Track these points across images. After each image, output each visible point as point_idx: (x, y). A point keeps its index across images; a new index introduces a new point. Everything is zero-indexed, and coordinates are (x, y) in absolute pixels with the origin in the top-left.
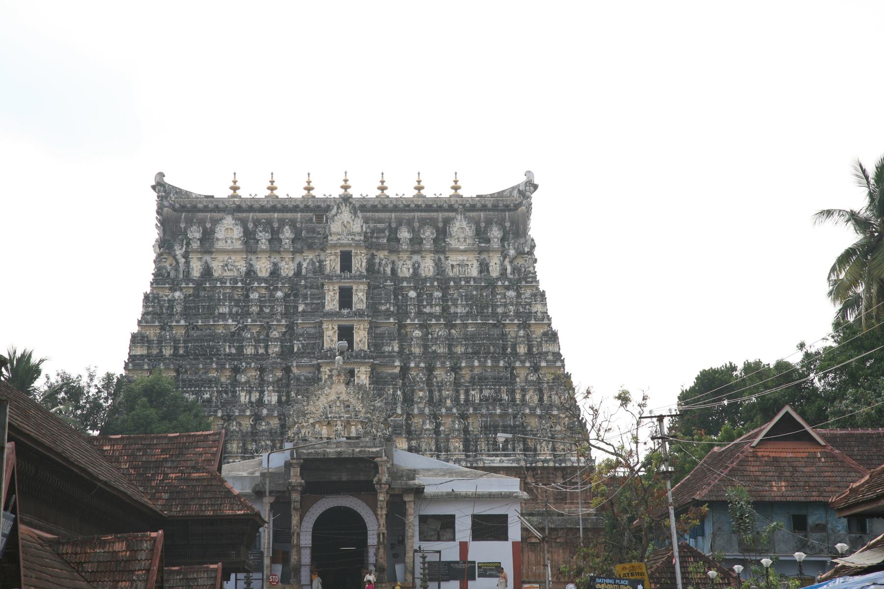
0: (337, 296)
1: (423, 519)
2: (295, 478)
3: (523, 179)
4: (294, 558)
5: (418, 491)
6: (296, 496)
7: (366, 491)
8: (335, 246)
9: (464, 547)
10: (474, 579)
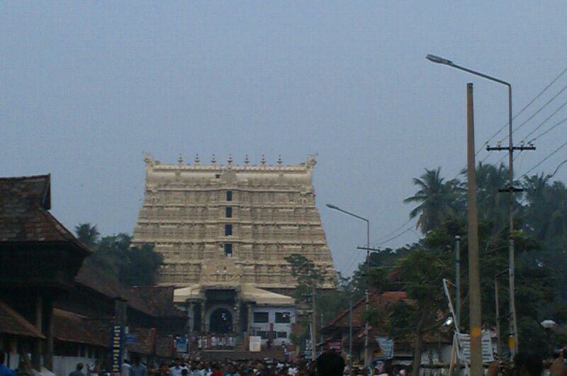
0: (225, 212)
1: (256, 314)
2: (202, 297)
3: (310, 159)
4: (202, 329)
5: (253, 304)
6: (203, 304)
7: (231, 302)
8: (224, 190)
9: (272, 325)
10: (275, 338)
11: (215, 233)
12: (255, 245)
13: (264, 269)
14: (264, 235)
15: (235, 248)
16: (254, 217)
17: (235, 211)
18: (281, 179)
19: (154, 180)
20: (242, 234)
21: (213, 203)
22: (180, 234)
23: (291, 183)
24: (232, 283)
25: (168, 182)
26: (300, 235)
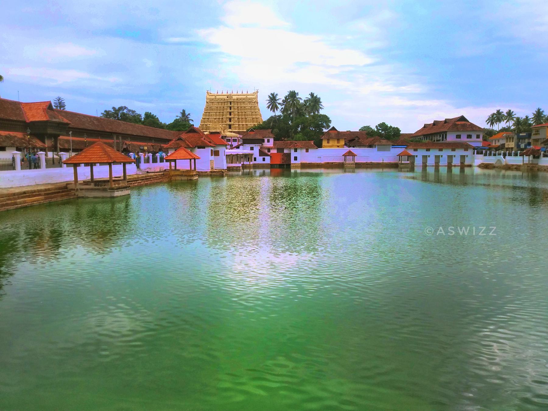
11: (226, 115)
12: (238, 118)
13: (241, 126)
14: (242, 115)
15: (232, 119)
16: (238, 110)
17: (232, 108)
18: (247, 98)
19: (209, 99)
20: (235, 115)
21: (226, 106)
22: (216, 115)
23: (249, 99)
24: (218, 131)
25: (213, 99)
26: (252, 115)
